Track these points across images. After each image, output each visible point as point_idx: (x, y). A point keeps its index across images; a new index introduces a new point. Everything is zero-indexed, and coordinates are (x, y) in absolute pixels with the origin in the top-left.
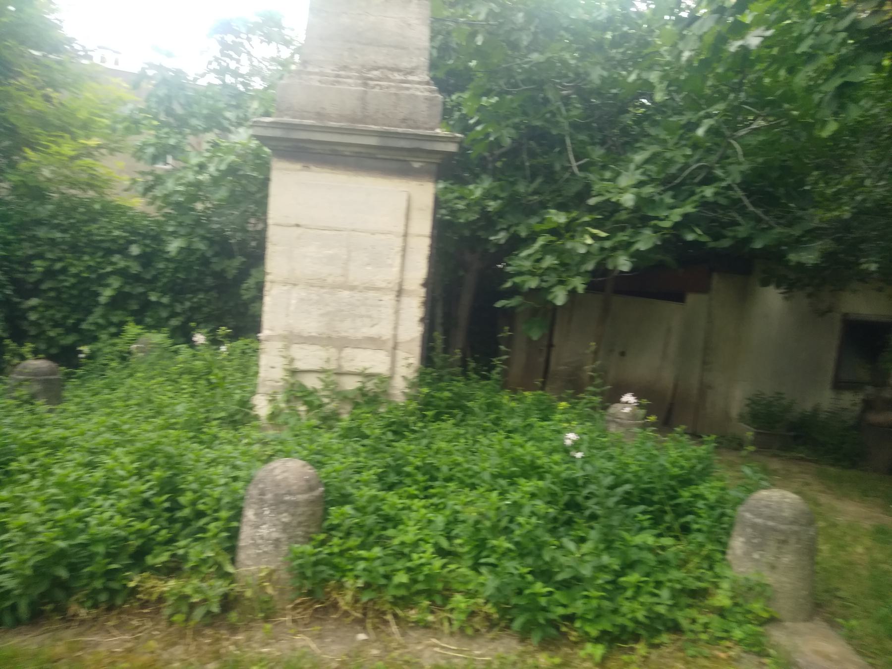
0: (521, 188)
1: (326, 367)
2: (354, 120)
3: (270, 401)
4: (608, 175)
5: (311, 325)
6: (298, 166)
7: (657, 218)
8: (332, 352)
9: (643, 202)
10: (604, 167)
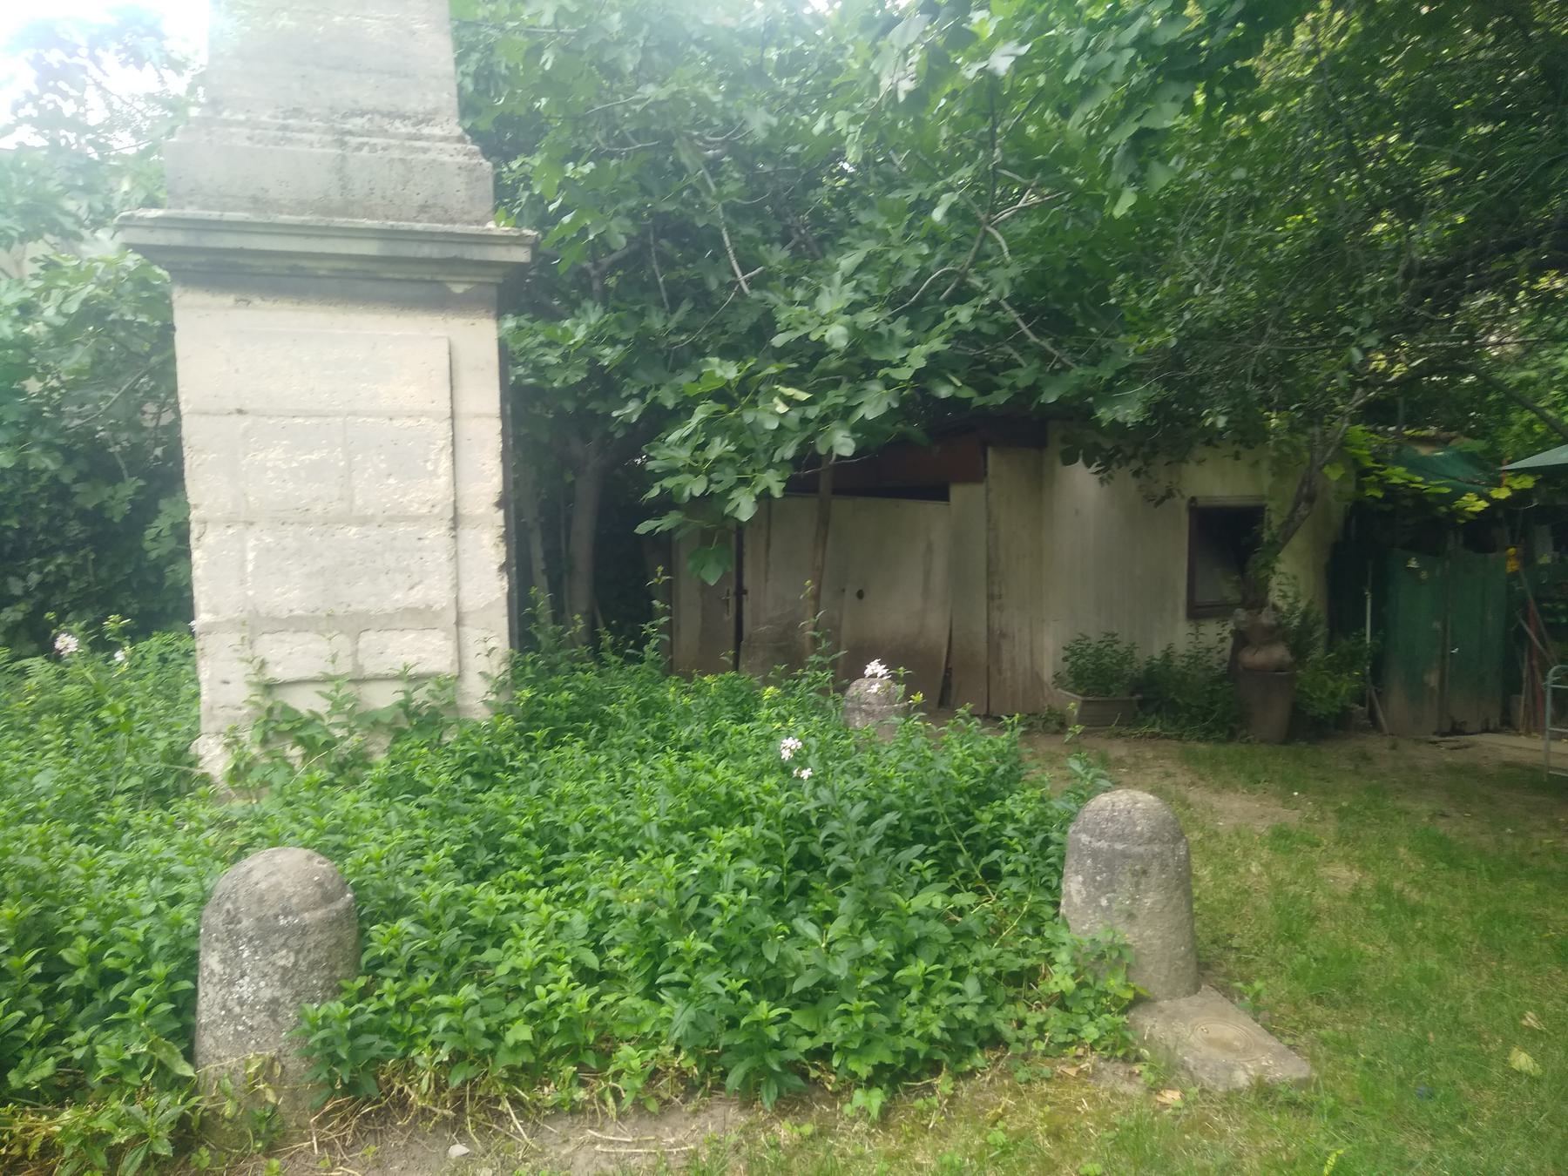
0: (656, 321)
1: (331, 671)
2: (328, 211)
3: (228, 745)
4: (799, 294)
6: (229, 300)
7: (888, 364)
8: (342, 642)
9: (862, 339)
10: (792, 281)
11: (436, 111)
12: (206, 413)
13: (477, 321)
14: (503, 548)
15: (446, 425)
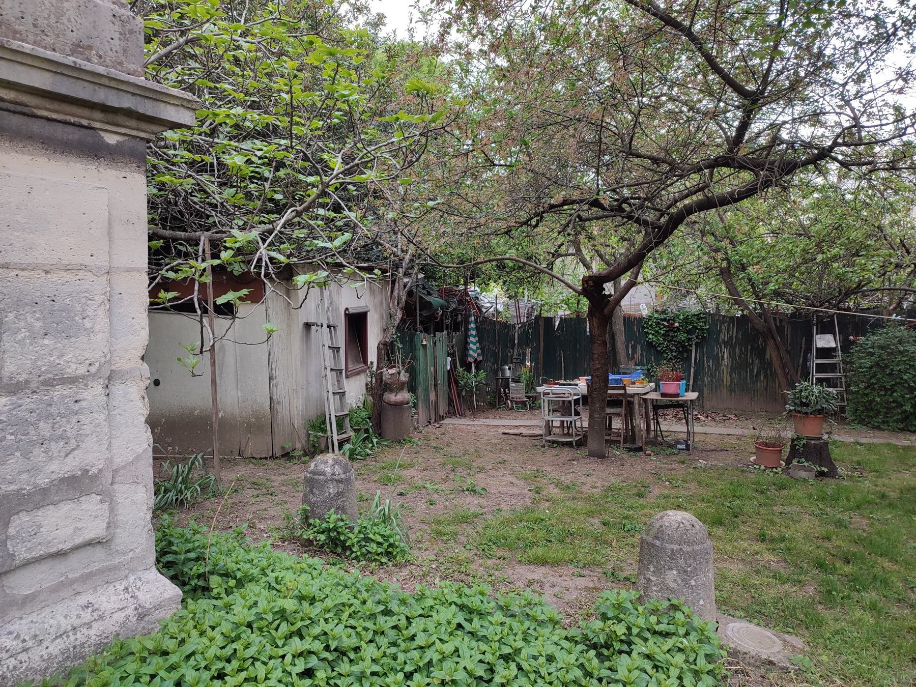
13: (128, 175)
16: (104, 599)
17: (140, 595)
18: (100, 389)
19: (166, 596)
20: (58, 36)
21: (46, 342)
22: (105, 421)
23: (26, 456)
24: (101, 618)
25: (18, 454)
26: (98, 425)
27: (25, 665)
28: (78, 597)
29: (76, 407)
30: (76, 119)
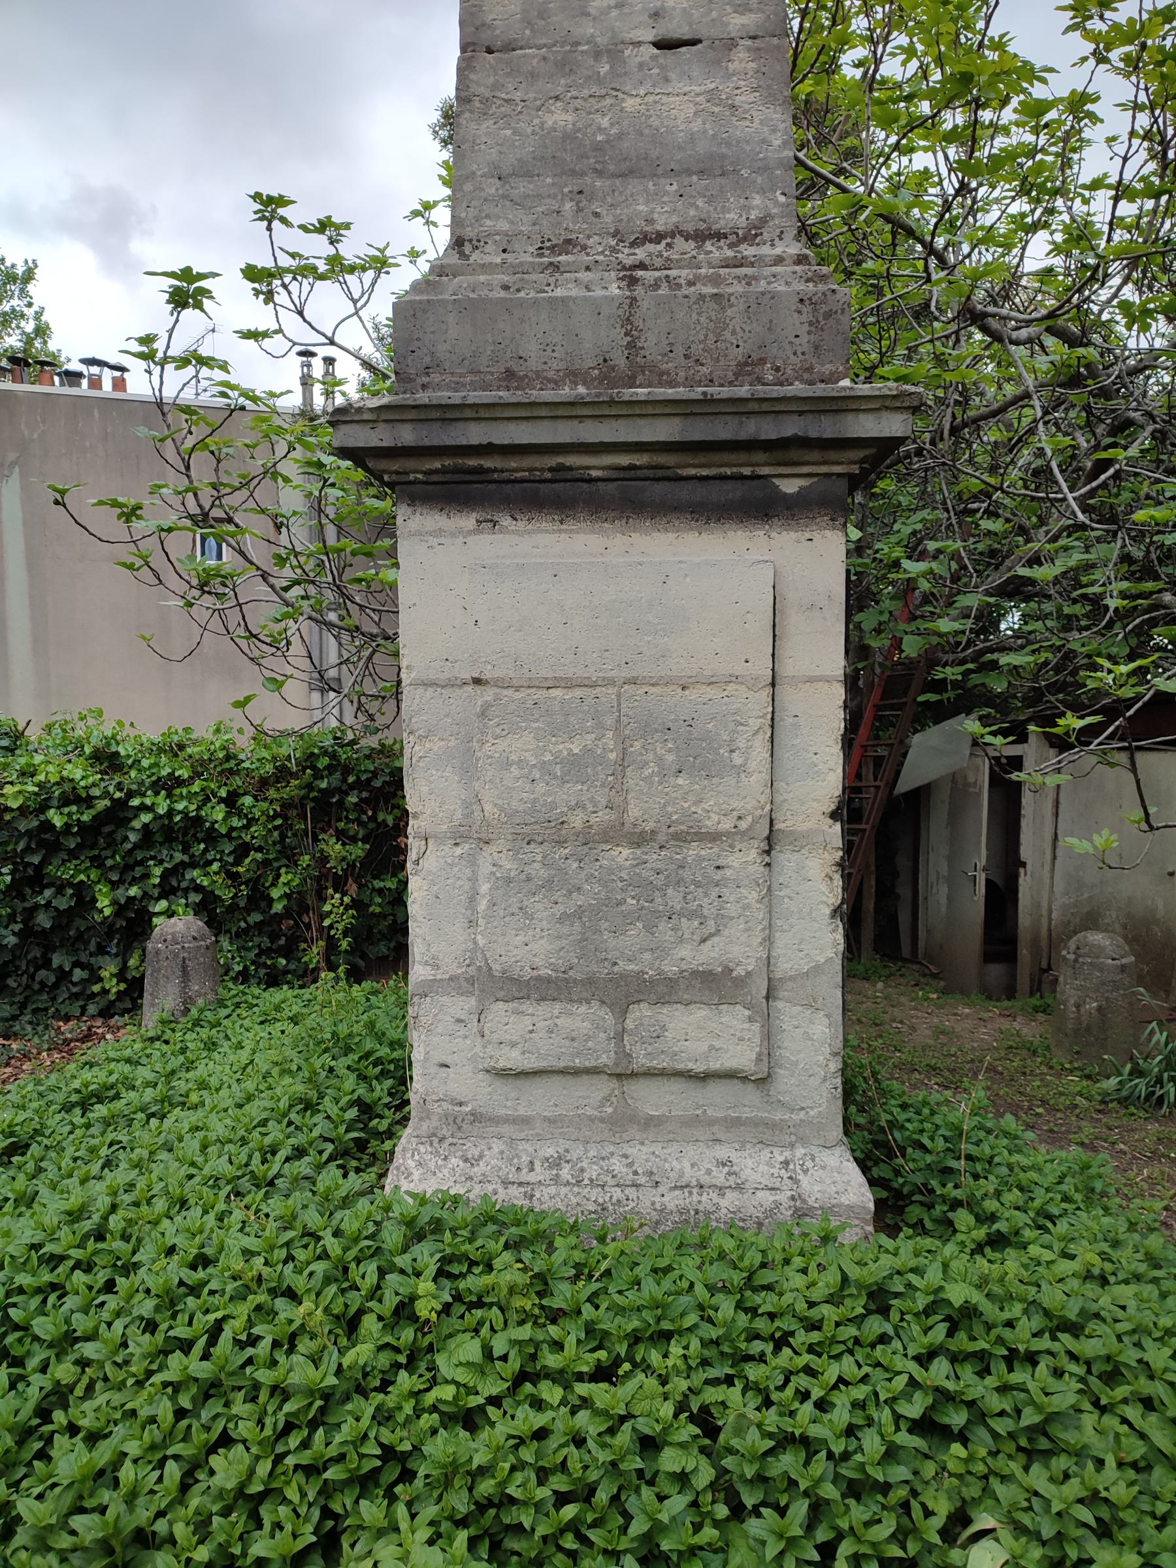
5: (532, 947)
6: (468, 521)
11: (763, 221)
12: (433, 684)
13: (816, 535)
14: (838, 882)
15: (765, 695)
16: (750, 1163)
17: (805, 1181)
18: (753, 854)
19: (845, 1200)
20: (718, 360)
21: (680, 781)
22: (760, 901)
23: (650, 929)
24: (739, 1187)
25: (640, 925)
26: (747, 907)
27: (632, 1204)
28: (718, 1147)
29: (718, 875)
30: (735, 470)
